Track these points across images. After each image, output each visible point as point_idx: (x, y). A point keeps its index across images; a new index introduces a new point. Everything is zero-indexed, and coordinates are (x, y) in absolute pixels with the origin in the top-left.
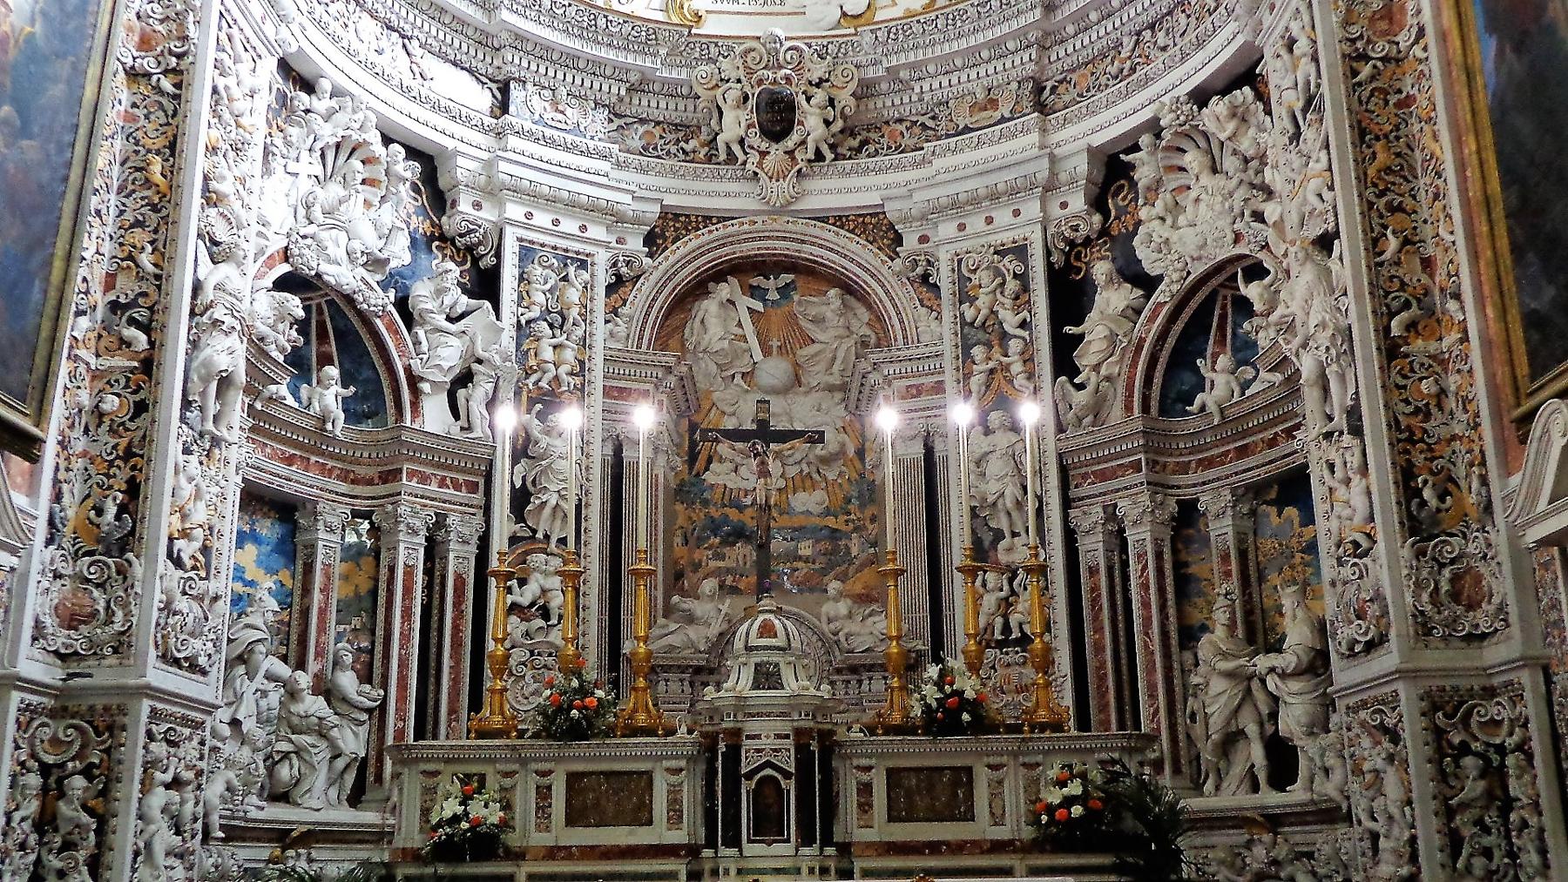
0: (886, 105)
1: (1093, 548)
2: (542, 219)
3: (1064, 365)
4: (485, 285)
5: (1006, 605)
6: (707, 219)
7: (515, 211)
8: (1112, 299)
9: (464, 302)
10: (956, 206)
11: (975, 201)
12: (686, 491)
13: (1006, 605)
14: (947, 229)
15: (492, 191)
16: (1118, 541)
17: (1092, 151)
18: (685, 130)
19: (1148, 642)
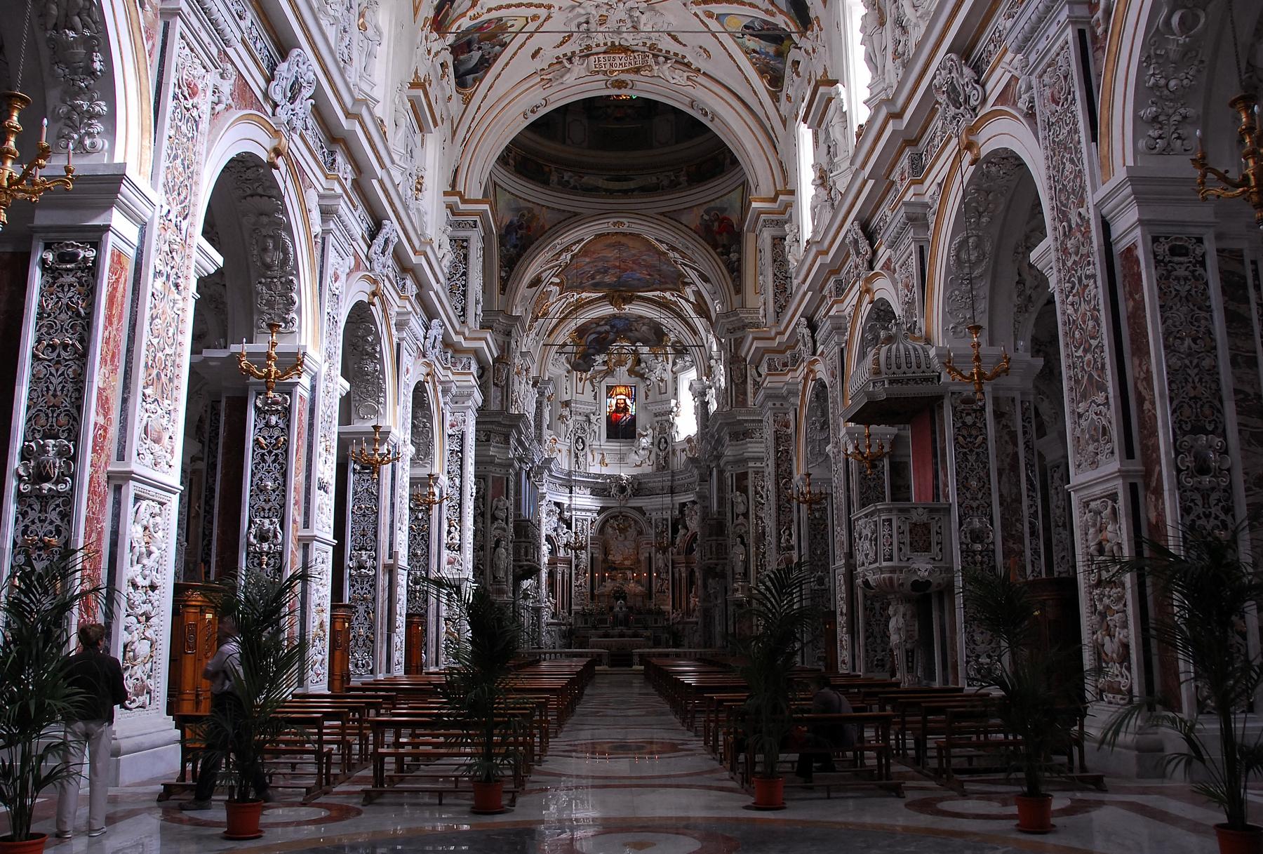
0: (643, 486)
1: (677, 575)
2: (579, 513)
3: (673, 543)
4: (569, 527)
5: (662, 585)
6: (609, 508)
7: (574, 513)
8: (682, 532)
9: (565, 530)
10: (656, 510)
11: (659, 509)
12: (605, 561)
13: (662, 585)
14: (654, 513)
15: (570, 509)
16: (680, 574)
17: (680, 504)
18: (605, 490)
19: (684, 594)
